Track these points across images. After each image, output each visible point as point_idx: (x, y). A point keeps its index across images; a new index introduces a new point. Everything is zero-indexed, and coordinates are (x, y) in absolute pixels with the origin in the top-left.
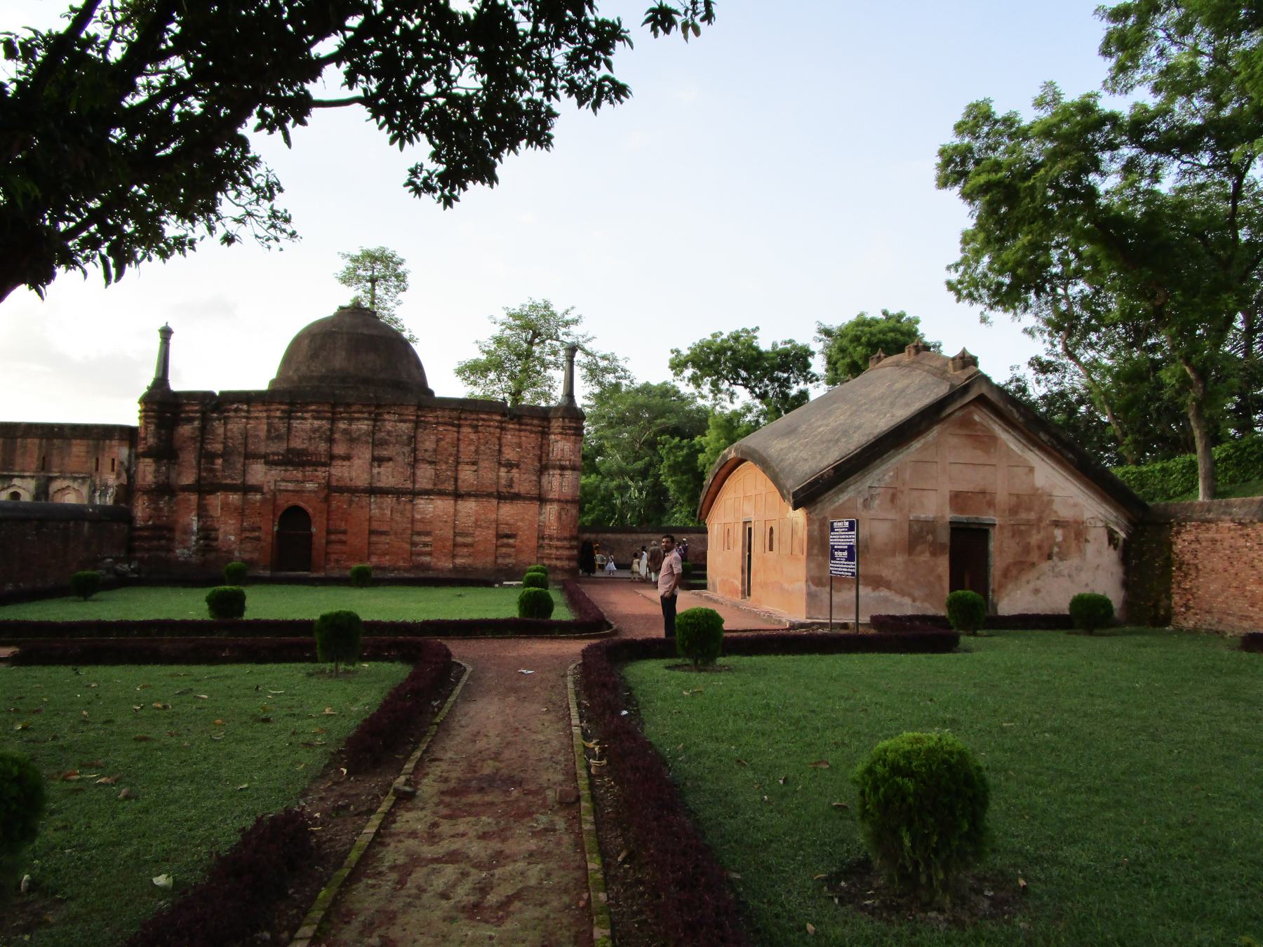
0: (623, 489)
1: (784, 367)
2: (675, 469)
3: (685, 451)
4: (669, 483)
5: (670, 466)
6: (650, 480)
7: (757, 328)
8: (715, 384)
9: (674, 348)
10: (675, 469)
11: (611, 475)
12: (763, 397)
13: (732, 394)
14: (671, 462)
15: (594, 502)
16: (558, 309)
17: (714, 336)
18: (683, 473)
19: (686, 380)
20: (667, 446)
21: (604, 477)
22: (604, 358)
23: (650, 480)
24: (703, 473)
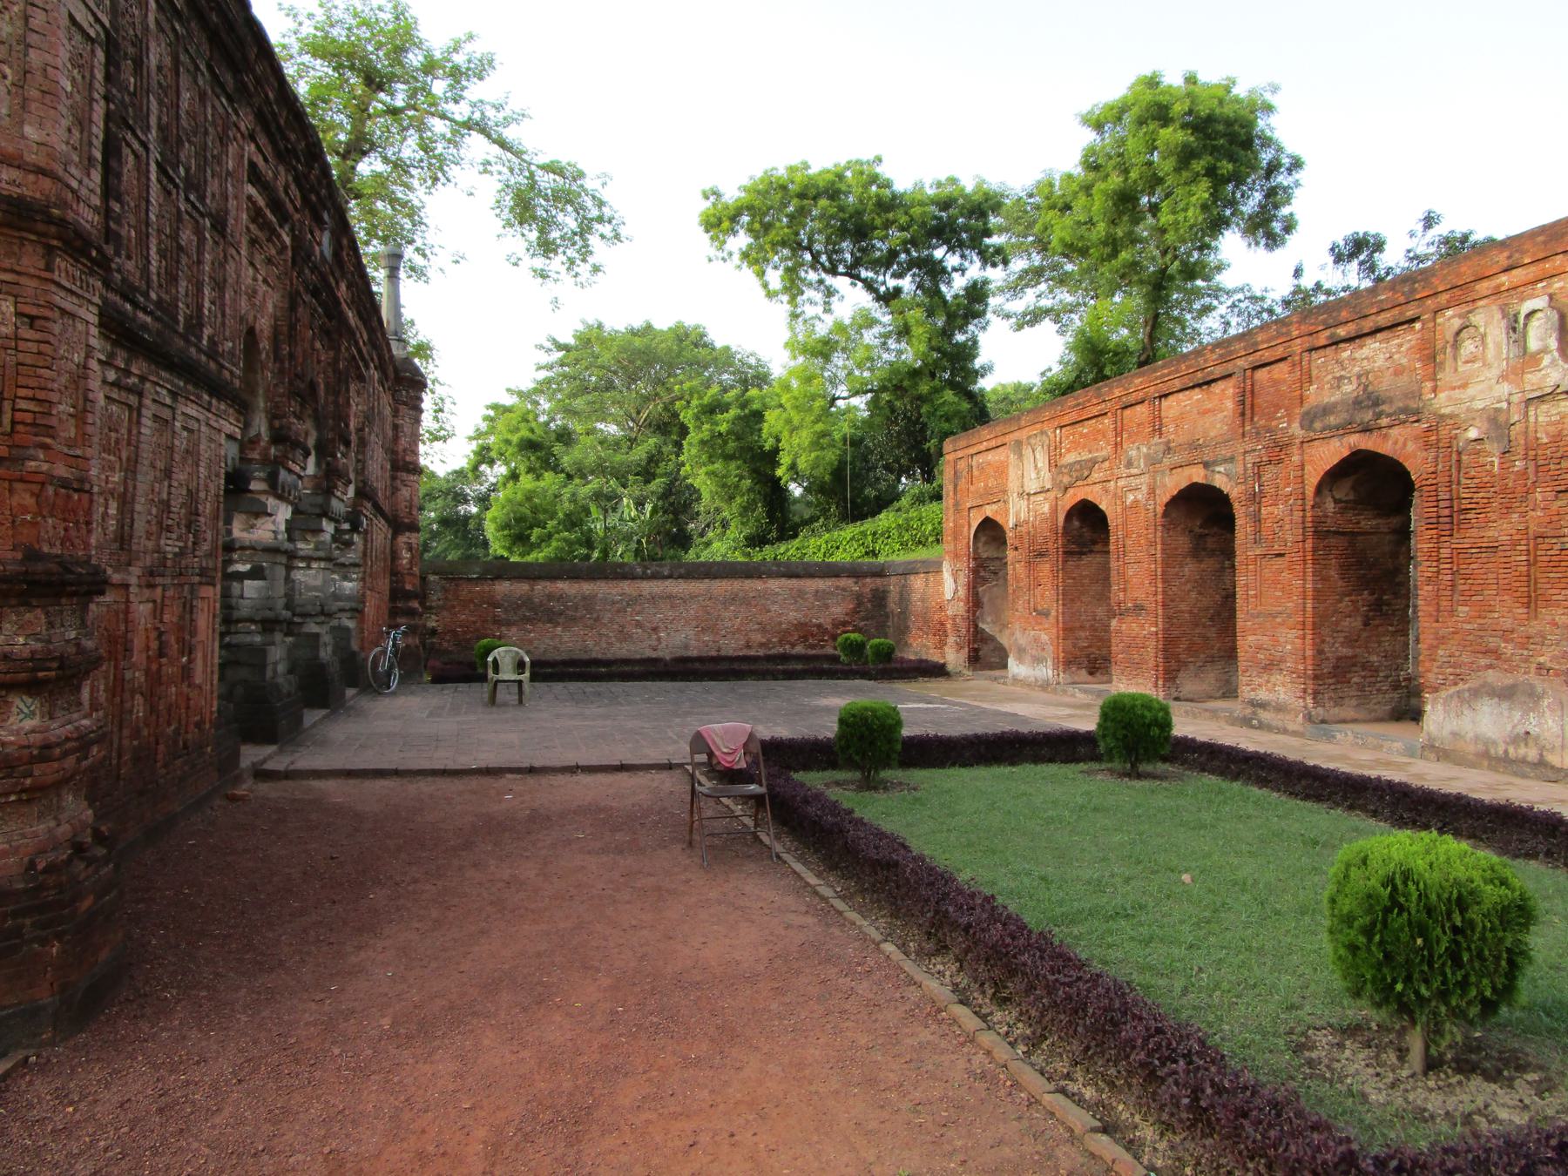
0: (608, 501)
1: (944, 232)
2: (714, 447)
3: (734, 412)
4: (701, 479)
5: (703, 442)
6: (657, 485)
7: (879, 160)
8: (792, 274)
9: (707, 188)
10: (714, 447)
11: (581, 472)
12: (889, 298)
13: (830, 292)
14: (705, 435)
15: (551, 524)
16: (435, 34)
17: (792, 169)
18: (728, 458)
19: (736, 257)
20: (695, 402)
21: (570, 477)
22: (552, 168)
23: (657, 485)
24: (776, 451)
